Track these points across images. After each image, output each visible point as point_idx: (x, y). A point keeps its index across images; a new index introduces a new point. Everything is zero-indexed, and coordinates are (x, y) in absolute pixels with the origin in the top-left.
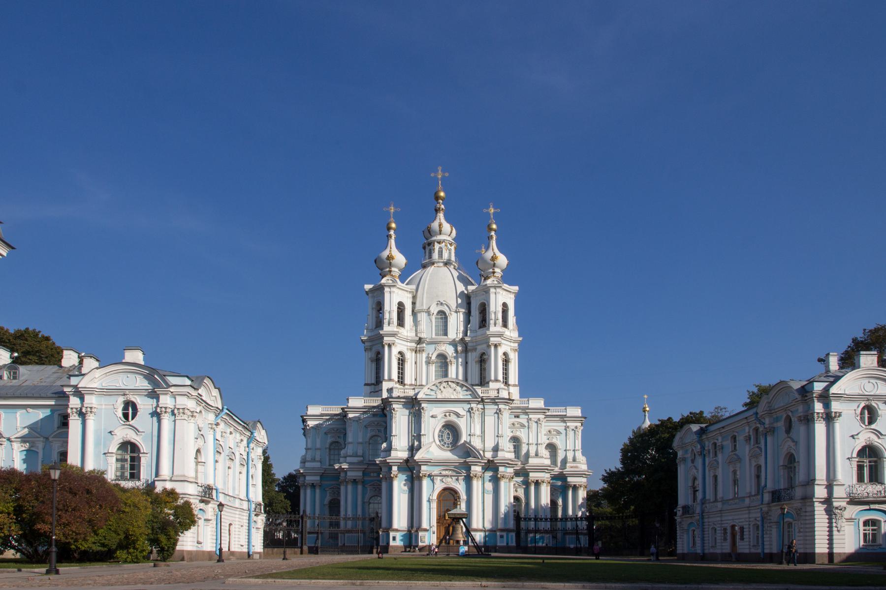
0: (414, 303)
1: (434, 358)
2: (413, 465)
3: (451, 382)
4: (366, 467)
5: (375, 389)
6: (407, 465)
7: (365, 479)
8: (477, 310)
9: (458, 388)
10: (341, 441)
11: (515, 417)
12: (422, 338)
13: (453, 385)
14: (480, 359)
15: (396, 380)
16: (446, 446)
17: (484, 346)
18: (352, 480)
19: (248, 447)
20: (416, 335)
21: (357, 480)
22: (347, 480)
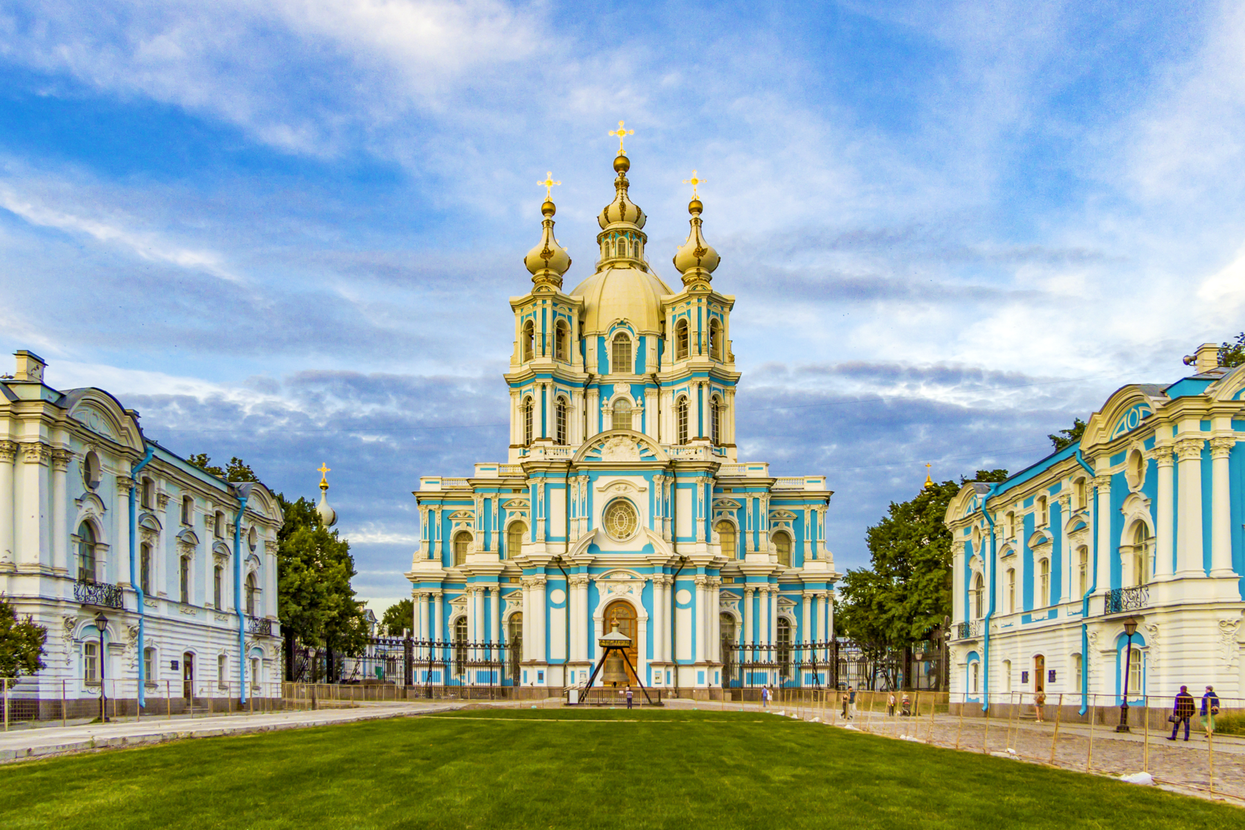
0: (581, 323)
3: (623, 436)
5: (524, 454)
9: (636, 447)
10: (470, 529)
12: (593, 375)
13: (627, 441)
18: (483, 589)
20: (585, 372)
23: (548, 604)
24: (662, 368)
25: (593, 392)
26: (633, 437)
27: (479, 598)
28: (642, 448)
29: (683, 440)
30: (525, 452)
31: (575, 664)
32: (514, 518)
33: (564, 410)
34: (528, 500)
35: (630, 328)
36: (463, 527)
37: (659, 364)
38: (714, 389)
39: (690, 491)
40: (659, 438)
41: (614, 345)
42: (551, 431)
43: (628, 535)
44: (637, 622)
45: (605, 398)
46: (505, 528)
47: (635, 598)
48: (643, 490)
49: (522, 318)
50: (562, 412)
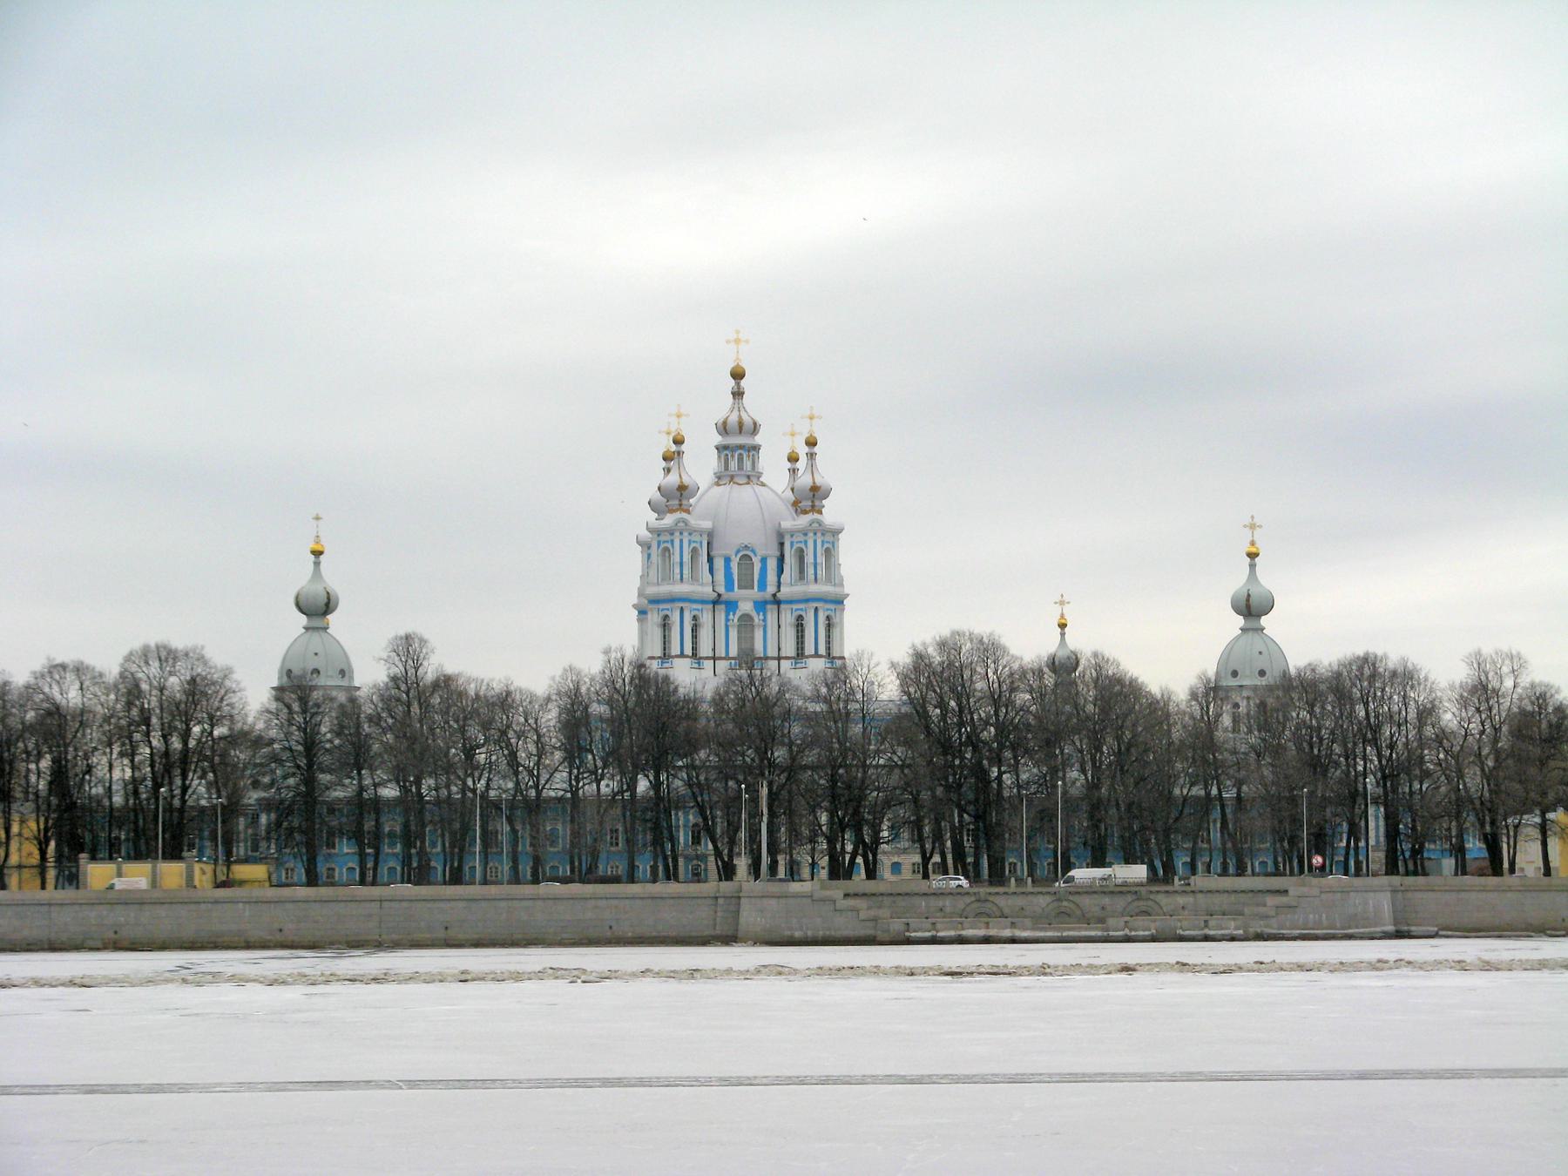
1: (736, 620)
15: (691, 654)
20: (713, 591)
24: (782, 588)
25: (721, 608)
29: (800, 654)
35: (753, 551)
38: (828, 610)
40: (779, 649)
50: (695, 629)
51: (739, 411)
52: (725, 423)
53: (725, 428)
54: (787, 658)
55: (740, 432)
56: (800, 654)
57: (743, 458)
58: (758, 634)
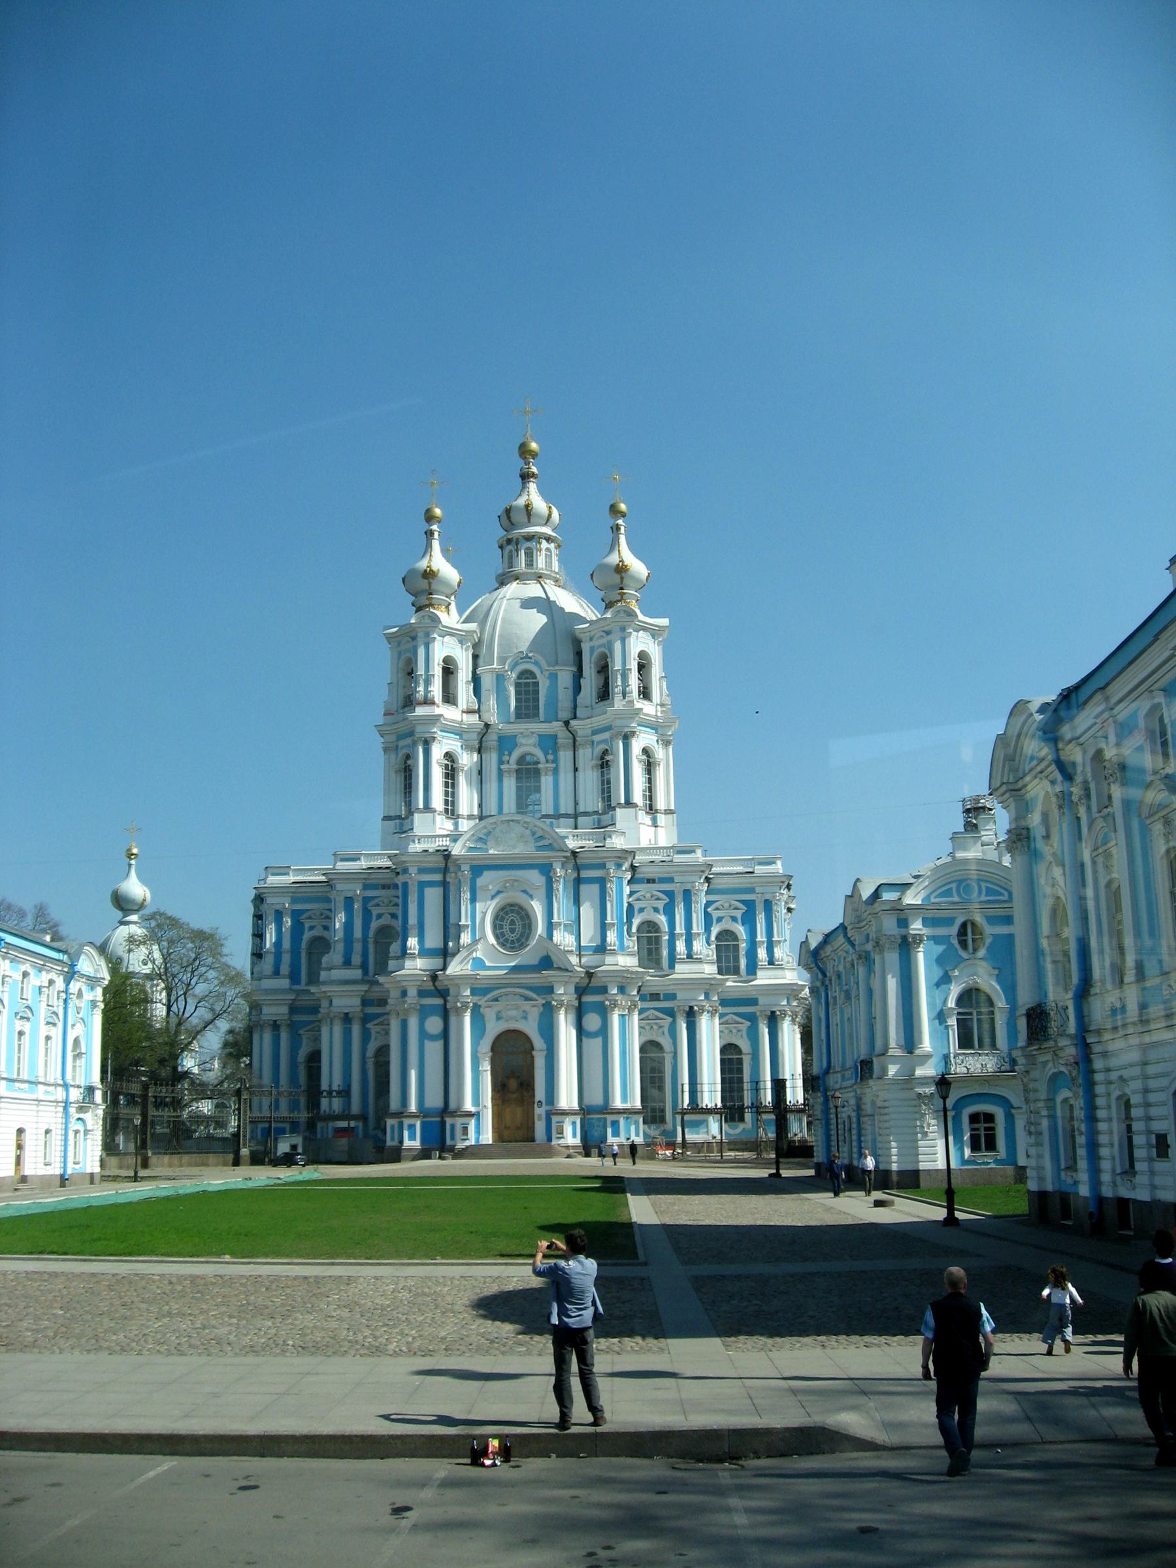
0: (475, 657)
2: (446, 985)
4: (366, 989)
6: (434, 985)
7: (366, 1012)
8: (593, 666)
10: (325, 934)
11: (649, 881)
12: (489, 725)
13: (518, 829)
14: (600, 763)
16: (508, 945)
17: (606, 735)
18: (342, 1016)
19: (66, 991)
21: (350, 1016)
22: (332, 1015)
23: (424, 1035)
26: (525, 822)
27: (338, 1029)
28: (537, 836)
30: (401, 825)
31: (454, 1114)
32: (382, 921)
33: (453, 769)
34: (398, 897)
35: (536, 663)
36: (316, 932)
37: (575, 707)
39: (595, 888)
40: (576, 804)
41: (517, 685)
42: (438, 801)
43: (521, 945)
44: (533, 1057)
45: (506, 753)
46: (371, 934)
47: (531, 1028)
48: (538, 888)
49: (400, 654)
51: (528, 495)
52: (508, 511)
53: (509, 518)
54: (586, 814)
55: (529, 521)
56: (609, 807)
57: (532, 553)
58: (546, 782)
